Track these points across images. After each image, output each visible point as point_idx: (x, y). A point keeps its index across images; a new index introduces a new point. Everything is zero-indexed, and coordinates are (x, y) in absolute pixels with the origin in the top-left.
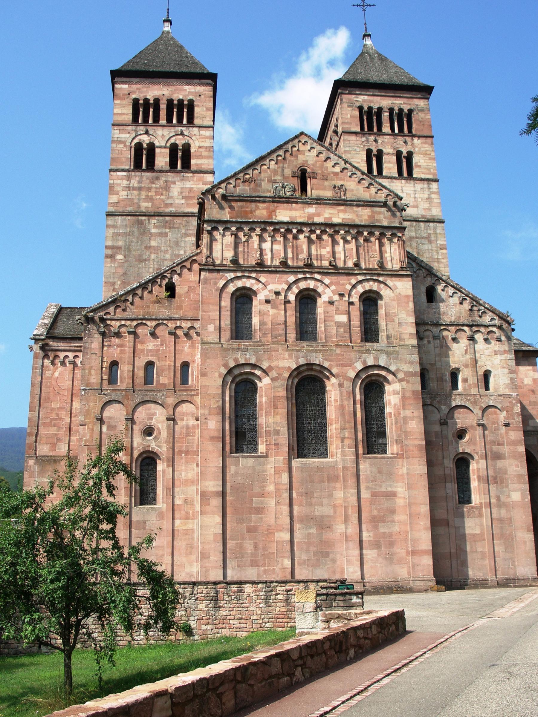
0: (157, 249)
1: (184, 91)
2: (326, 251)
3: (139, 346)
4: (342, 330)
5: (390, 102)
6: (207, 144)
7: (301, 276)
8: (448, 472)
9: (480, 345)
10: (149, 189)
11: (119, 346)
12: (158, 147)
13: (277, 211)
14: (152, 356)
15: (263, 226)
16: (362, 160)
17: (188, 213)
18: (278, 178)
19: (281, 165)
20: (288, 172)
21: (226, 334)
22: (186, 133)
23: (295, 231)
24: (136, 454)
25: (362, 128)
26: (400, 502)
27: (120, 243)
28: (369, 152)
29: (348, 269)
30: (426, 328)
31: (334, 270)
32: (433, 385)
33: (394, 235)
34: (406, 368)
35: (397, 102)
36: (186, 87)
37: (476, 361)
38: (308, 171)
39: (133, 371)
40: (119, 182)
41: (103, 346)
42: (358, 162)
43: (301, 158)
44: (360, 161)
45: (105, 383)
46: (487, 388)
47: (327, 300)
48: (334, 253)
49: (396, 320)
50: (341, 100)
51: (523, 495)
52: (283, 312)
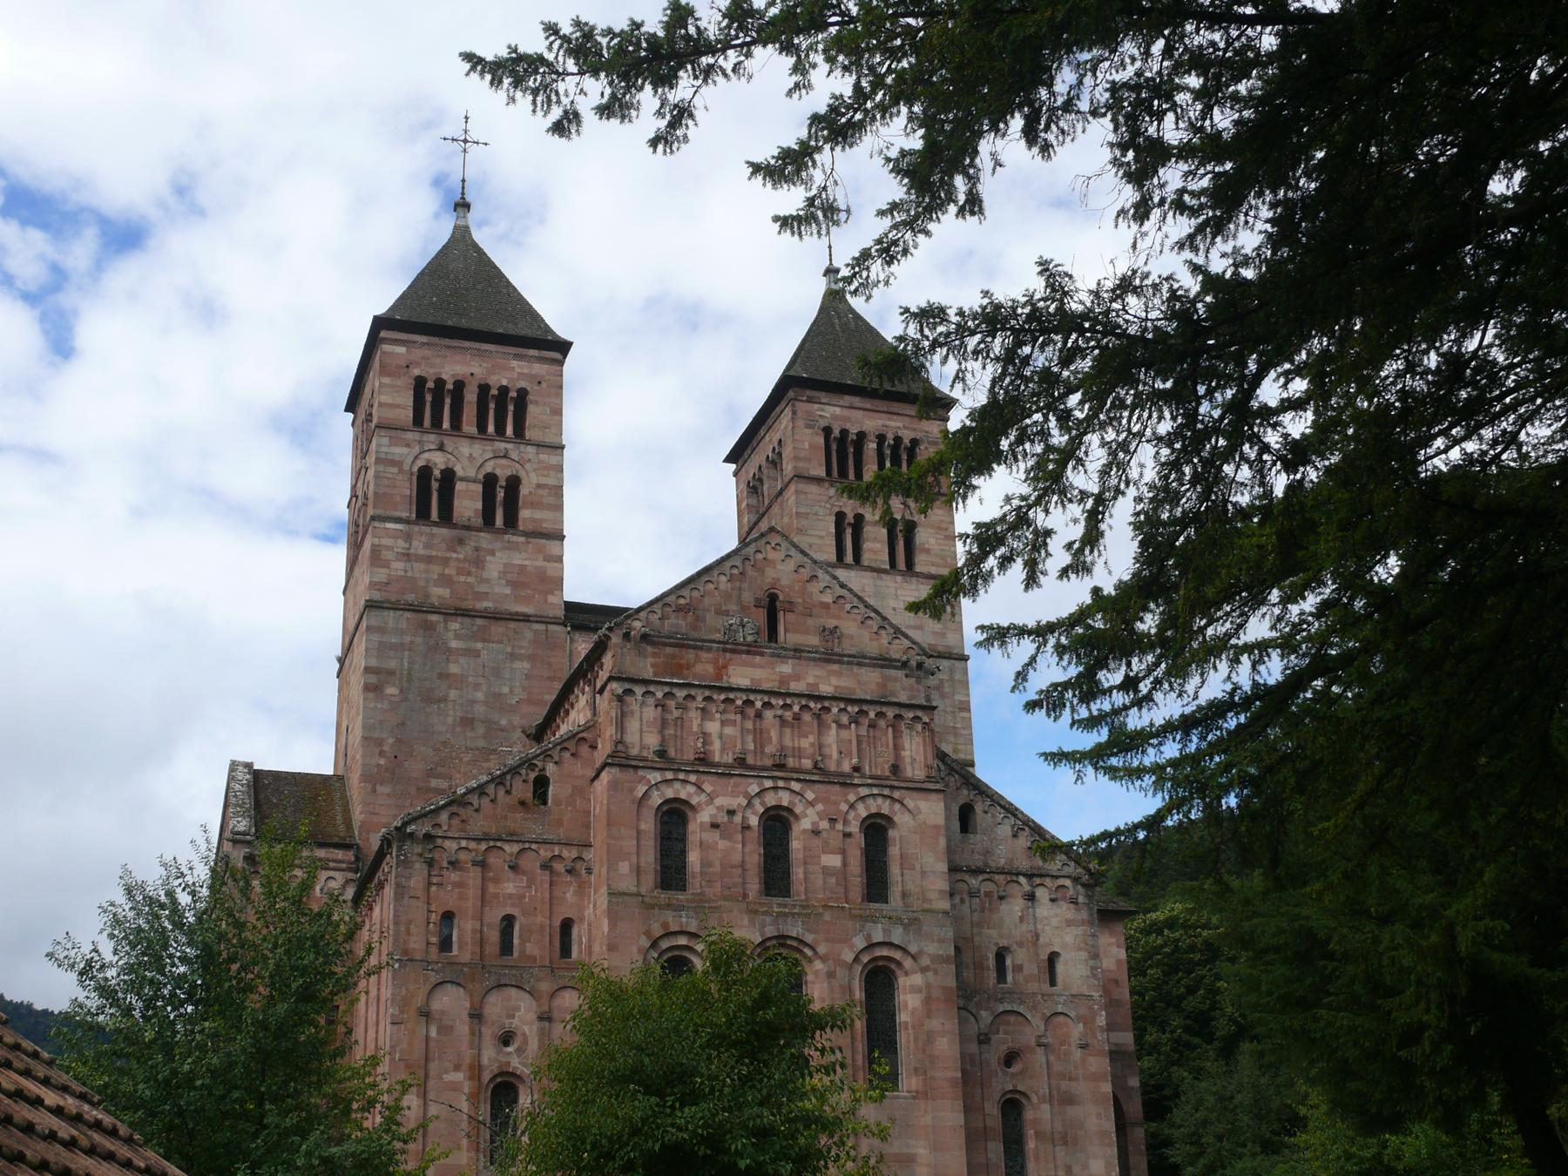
0: (459, 681)
1: (511, 370)
3: (491, 889)
4: (833, 880)
5: (880, 422)
6: (551, 481)
7: (768, 784)
8: (990, 1123)
9: (1044, 909)
11: (455, 885)
12: (462, 479)
14: (513, 905)
15: (707, 693)
17: (517, 614)
18: (733, 607)
20: (748, 597)
21: (649, 880)
22: (514, 455)
23: (759, 704)
24: (486, 1077)
27: (392, 664)
29: (842, 775)
30: (958, 876)
31: (822, 775)
32: (968, 974)
33: (916, 718)
34: (932, 948)
35: (893, 424)
36: (514, 363)
37: (1037, 936)
39: (481, 932)
41: (430, 884)
42: (821, 537)
43: (770, 573)
45: (434, 950)
46: (1053, 983)
48: (821, 746)
49: (918, 866)
50: (794, 413)
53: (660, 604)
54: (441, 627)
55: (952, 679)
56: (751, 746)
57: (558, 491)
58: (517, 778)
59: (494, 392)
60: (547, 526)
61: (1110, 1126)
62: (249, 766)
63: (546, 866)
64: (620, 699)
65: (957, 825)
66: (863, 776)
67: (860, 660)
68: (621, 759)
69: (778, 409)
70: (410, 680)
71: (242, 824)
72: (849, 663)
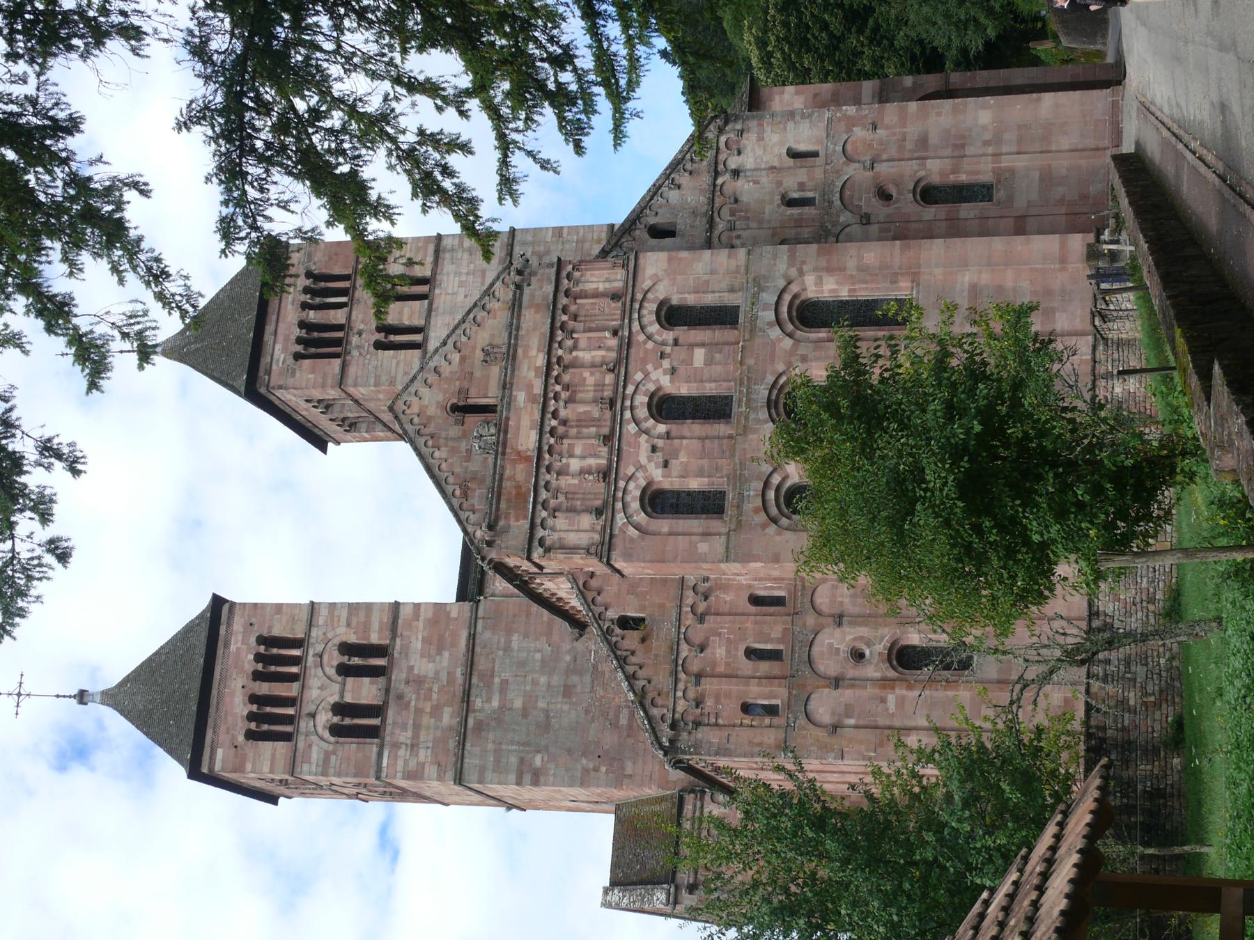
0: (530, 700)
1: (239, 651)
2: (590, 378)
3: (721, 669)
4: (717, 356)
5: (290, 307)
6: (344, 614)
7: (628, 414)
8: (942, 215)
9: (748, 161)
10: (419, 711)
11: (717, 701)
13: (520, 448)
14: (737, 650)
16: (394, 357)
18: (463, 446)
19: (442, 441)
20: (455, 431)
21: (715, 524)
22: (320, 648)
23: (554, 423)
24: (892, 674)
25: (337, 356)
26: (985, 278)
27: (514, 760)
28: (379, 346)
29: (621, 346)
30: (715, 240)
31: (620, 365)
32: (806, 232)
33: (569, 277)
34: (782, 266)
36: (233, 648)
37: (773, 168)
38: (455, 401)
39: (760, 678)
40: (400, 763)
41: (716, 725)
43: (432, 411)
44: (394, 362)
45: (776, 721)
46: (815, 154)
47: (668, 377)
48: (593, 365)
49: (706, 277)
50: (280, 387)
51: (984, 107)
52: (685, 441)
53: (460, 513)
54: (480, 716)
55: (533, 243)
56: (593, 430)
57: (353, 608)
58: (618, 645)
59: (260, 667)
60: (386, 618)
61: (947, 104)
62: (606, 891)
63: (701, 619)
64: (548, 550)
65: (668, 241)
66: (622, 327)
67: (514, 328)
68: (604, 549)
69: (277, 402)
70: (527, 744)
71: (660, 896)
72: (517, 338)
